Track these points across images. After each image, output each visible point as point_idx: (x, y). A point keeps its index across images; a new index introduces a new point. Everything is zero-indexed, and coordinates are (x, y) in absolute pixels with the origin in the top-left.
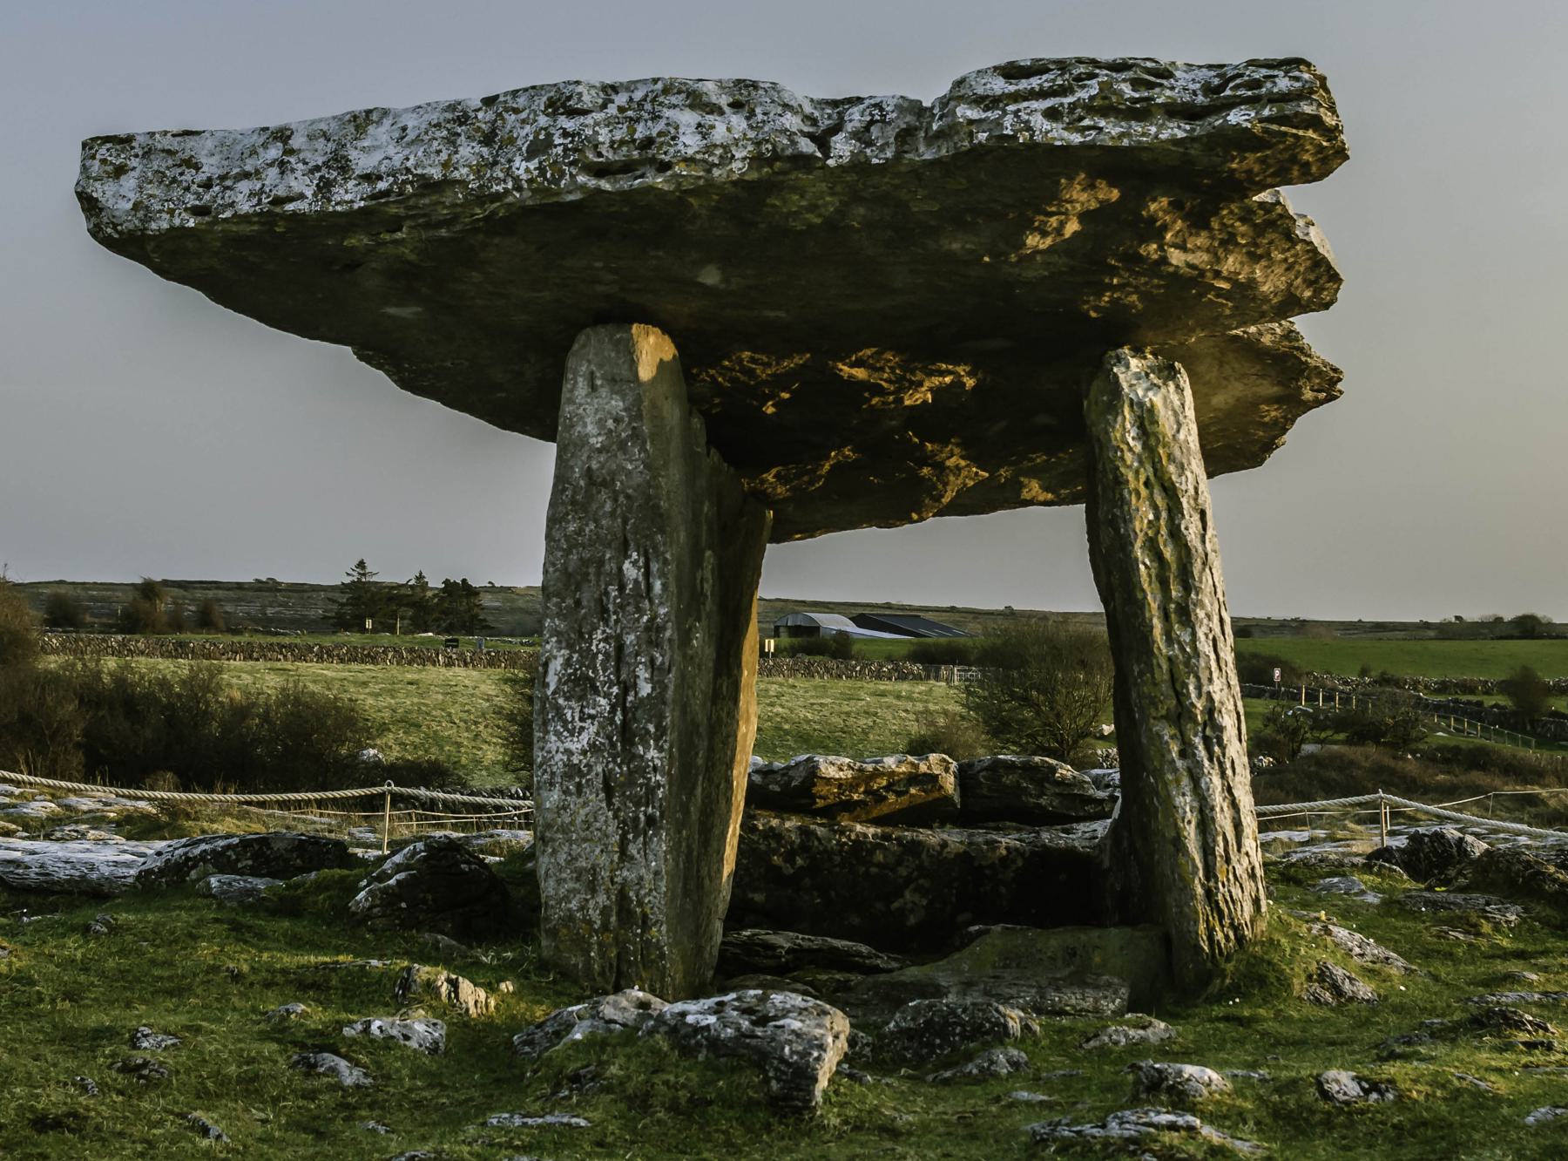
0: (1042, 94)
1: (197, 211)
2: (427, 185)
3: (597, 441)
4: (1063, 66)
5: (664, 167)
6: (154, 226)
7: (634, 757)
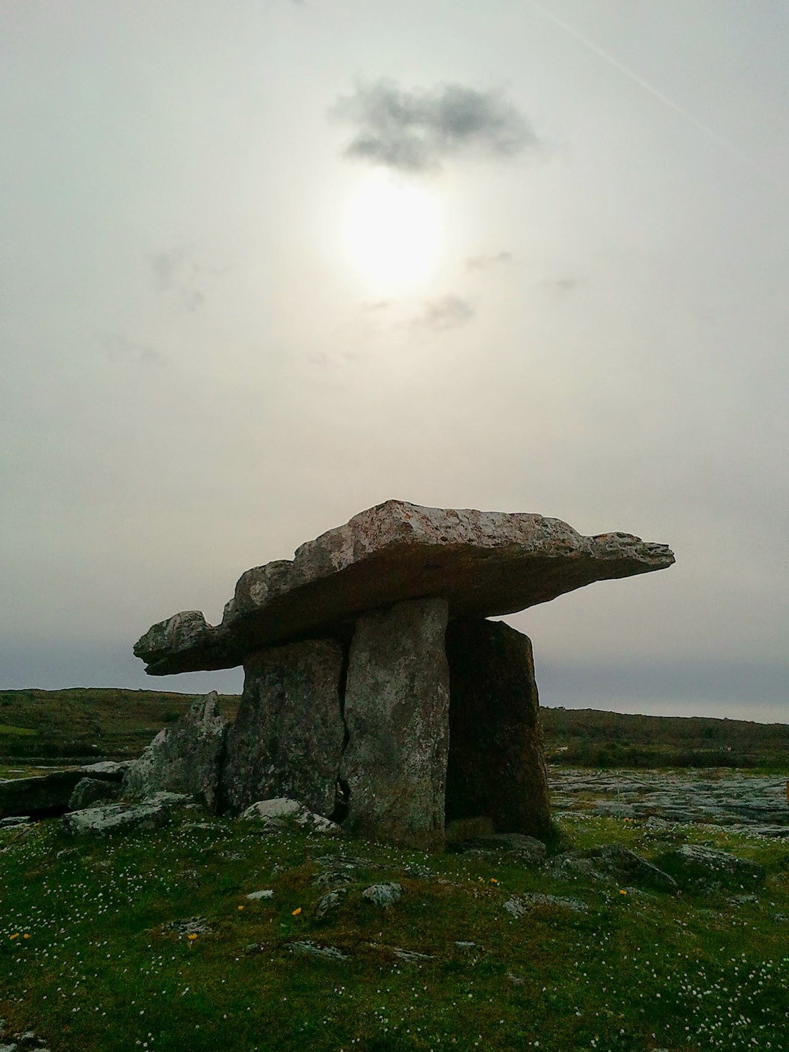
0: (630, 545)
1: (444, 539)
2: (512, 544)
3: (431, 640)
4: (630, 536)
5: (571, 550)
6: (430, 542)
7: (439, 761)
